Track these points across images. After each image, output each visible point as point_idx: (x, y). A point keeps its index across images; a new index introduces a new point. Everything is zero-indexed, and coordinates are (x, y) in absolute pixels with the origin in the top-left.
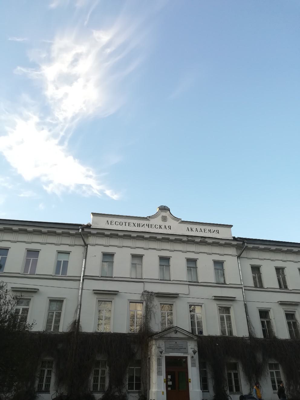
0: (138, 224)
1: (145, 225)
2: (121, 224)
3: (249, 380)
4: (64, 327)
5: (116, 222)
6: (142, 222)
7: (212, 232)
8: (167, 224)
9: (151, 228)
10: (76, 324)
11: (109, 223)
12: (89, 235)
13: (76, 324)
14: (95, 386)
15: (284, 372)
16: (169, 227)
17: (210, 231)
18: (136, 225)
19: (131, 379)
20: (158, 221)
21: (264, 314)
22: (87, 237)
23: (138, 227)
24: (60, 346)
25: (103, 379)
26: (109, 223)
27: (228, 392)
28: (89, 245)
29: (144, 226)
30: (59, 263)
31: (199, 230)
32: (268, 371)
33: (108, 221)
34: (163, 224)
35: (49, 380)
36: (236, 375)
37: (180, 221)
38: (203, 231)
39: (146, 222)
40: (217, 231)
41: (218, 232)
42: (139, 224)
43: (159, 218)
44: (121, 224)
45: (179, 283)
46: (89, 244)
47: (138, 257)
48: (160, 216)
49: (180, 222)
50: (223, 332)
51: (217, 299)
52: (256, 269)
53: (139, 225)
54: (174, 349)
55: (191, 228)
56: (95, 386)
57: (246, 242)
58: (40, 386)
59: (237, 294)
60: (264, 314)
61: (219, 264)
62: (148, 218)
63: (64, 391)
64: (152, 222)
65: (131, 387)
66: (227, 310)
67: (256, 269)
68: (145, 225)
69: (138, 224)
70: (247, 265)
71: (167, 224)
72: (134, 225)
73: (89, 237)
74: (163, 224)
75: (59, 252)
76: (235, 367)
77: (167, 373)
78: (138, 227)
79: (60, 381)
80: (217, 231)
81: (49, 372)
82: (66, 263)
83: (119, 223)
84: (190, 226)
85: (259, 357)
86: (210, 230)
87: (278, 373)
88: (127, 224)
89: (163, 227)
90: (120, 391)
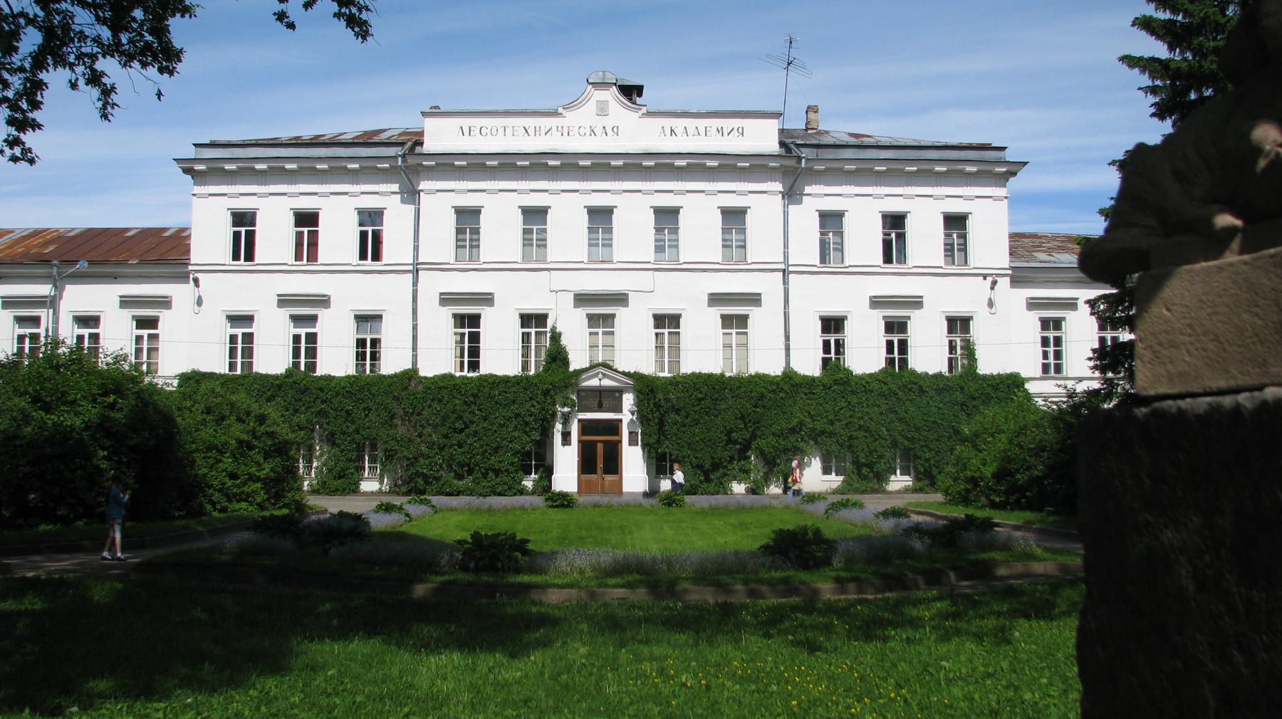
0: (535, 127)
1: (554, 129)
2: (494, 131)
5: (481, 128)
7: (725, 134)
8: (609, 122)
9: (568, 135)
11: (466, 131)
12: (419, 169)
16: (615, 129)
17: (720, 131)
18: (531, 131)
21: (832, 324)
22: (418, 173)
23: (535, 135)
26: (466, 131)
28: (421, 193)
29: (550, 132)
31: (691, 131)
33: (461, 128)
34: (598, 123)
37: (644, 110)
38: (702, 133)
40: (740, 130)
41: (743, 134)
42: (538, 129)
44: (494, 131)
46: (422, 191)
47: (534, 215)
49: (643, 114)
51: (716, 299)
52: (831, 221)
55: (671, 128)
57: (804, 158)
59: (768, 286)
61: (734, 217)
62: (560, 110)
67: (831, 221)
68: (554, 129)
69: (535, 127)
70: (805, 217)
71: (609, 122)
72: (527, 132)
73: (422, 174)
74: (598, 123)
78: (535, 135)
80: (740, 130)
83: (489, 129)
84: (669, 122)
86: (722, 128)
88: (509, 131)
89: (598, 130)
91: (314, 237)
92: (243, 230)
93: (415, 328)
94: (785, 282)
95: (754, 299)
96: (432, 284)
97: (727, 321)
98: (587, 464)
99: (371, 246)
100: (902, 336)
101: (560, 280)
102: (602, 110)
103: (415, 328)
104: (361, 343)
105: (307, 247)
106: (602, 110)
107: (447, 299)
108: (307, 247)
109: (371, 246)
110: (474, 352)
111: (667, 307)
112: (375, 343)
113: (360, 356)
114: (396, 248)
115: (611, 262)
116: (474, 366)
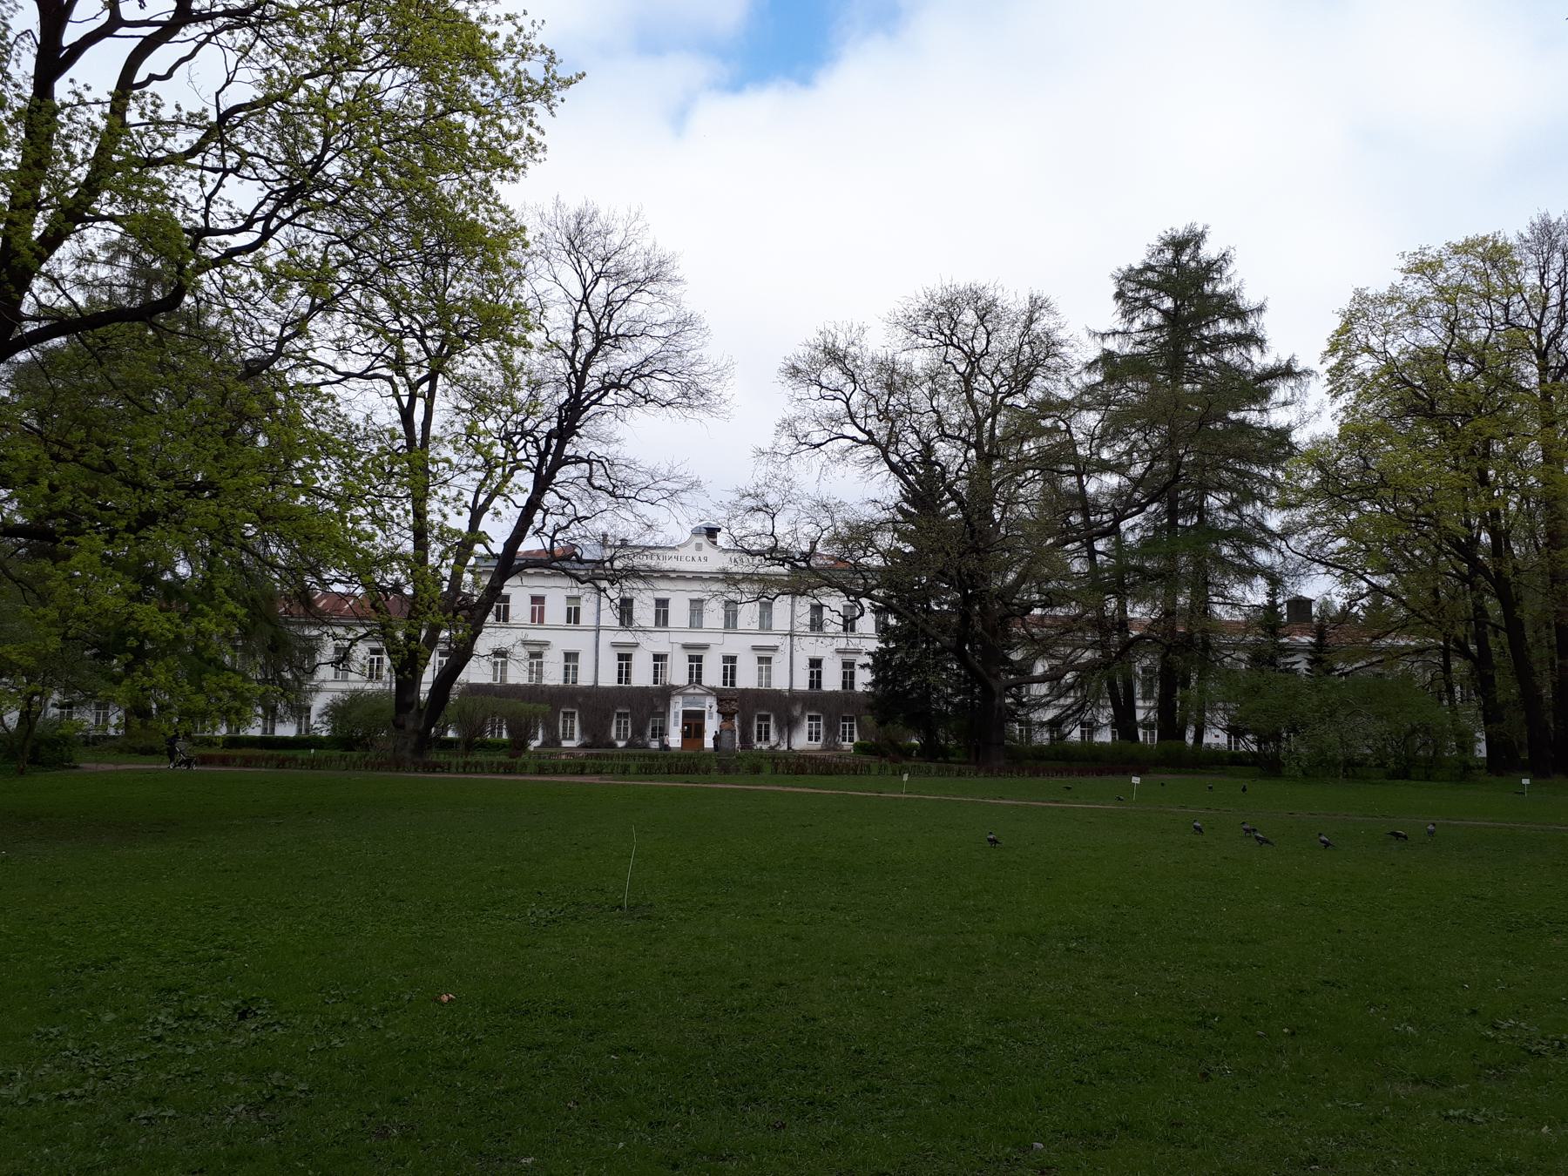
3: (780, 731)
8: (702, 554)
15: (825, 724)
19: (654, 729)
20: (690, 551)
21: (816, 663)
25: (626, 729)
27: (755, 740)
30: (569, 610)
32: (806, 723)
34: (697, 554)
35: (572, 729)
36: (767, 727)
43: (693, 545)
45: (713, 631)
48: (694, 543)
50: (760, 684)
51: (755, 648)
54: (691, 704)
58: (564, 734)
60: (816, 663)
63: (587, 739)
64: (682, 552)
65: (654, 736)
66: (769, 660)
71: (702, 554)
74: (697, 554)
75: (568, 598)
76: (767, 718)
77: (684, 725)
79: (583, 731)
81: (572, 722)
82: (577, 610)
85: (797, 712)
87: (818, 726)
90: (643, 739)
91: (542, 610)
93: (597, 660)
94: (792, 641)
95: (775, 649)
96: (606, 638)
97: (760, 660)
98: (685, 735)
99: (573, 616)
101: (676, 638)
102: (699, 547)
103: (597, 660)
104: (567, 668)
105: (538, 615)
106: (699, 547)
107: (615, 645)
108: (538, 615)
109: (573, 616)
111: (731, 652)
112: (575, 668)
113: (566, 675)
114: (587, 617)
115: (701, 628)
116: (628, 681)
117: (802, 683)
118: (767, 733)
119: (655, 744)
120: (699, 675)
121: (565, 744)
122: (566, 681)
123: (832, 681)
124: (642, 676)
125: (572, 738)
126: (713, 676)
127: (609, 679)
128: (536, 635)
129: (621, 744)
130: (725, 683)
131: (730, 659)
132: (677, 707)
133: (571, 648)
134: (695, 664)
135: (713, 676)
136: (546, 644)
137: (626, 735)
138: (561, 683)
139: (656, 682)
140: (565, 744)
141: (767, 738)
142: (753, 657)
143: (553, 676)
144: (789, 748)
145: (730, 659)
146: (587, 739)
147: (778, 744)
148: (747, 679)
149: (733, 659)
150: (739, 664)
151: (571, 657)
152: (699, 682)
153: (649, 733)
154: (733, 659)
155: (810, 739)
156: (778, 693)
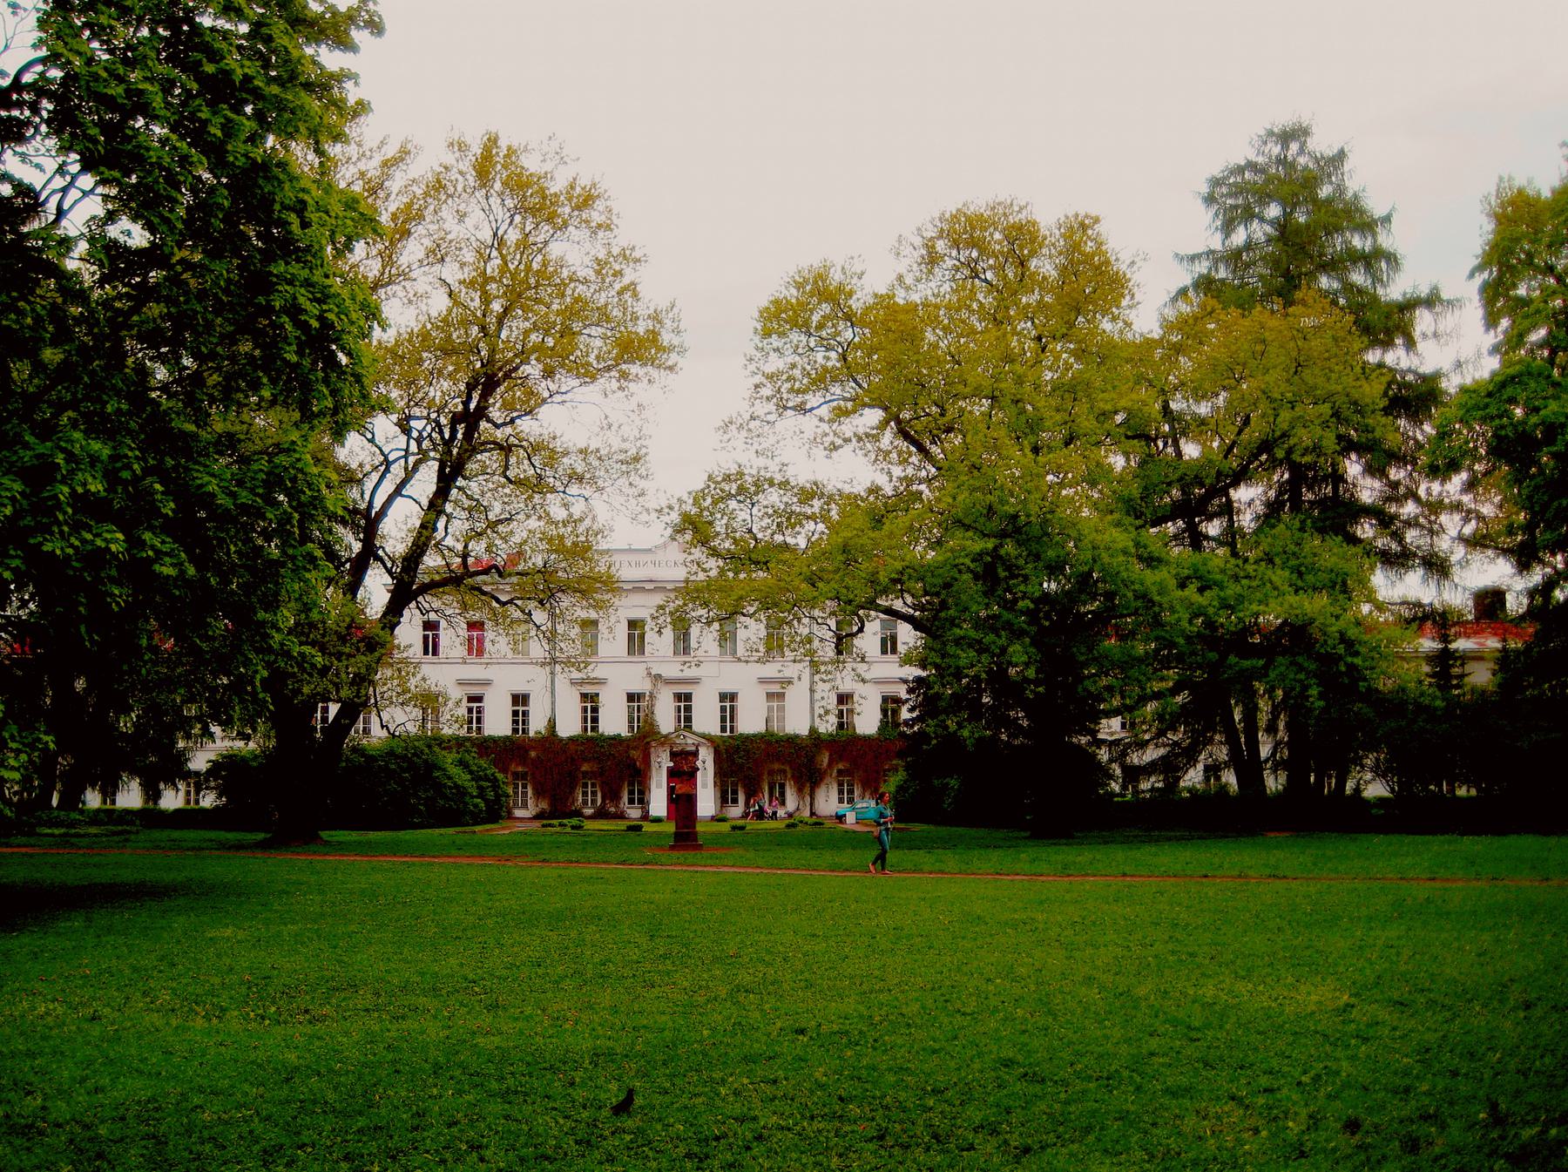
3: (800, 791)
4: (537, 725)
6: (643, 558)
10: (552, 724)
13: (552, 724)
14: (585, 802)
24: (533, 754)
35: (525, 794)
36: (782, 787)
39: (649, 557)
53: (637, 564)
56: (585, 802)
63: (544, 805)
64: (660, 556)
65: (631, 801)
66: (781, 696)
79: (538, 794)
81: (524, 786)
90: (617, 806)
92: (430, 633)
93: (553, 703)
97: (770, 696)
100: (849, 707)
103: (553, 703)
104: (515, 713)
110: (595, 720)
111: (728, 688)
112: (525, 714)
113: (515, 722)
117: (827, 726)
118: (782, 794)
119: (634, 813)
120: (688, 719)
121: (518, 813)
122: (515, 731)
123: (867, 722)
124: (614, 722)
125: (525, 806)
126: (707, 720)
127: (569, 727)
128: (475, 671)
129: (589, 811)
130: (723, 729)
131: (728, 698)
132: (661, 764)
133: (520, 688)
134: (682, 704)
135: (707, 720)
136: (487, 683)
137: (593, 802)
138: (509, 733)
139: (631, 728)
140: (518, 813)
141: (783, 803)
142: (760, 693)
143: (497, 724)
144: (813, 814)
145: (728, 698)
146: (544, 805)
147: (798, 809)
148: (751, 722)
149: (732, 697)
150: (741, 704)
151: (520, 699)
152: (688, 727)
153: (625, 798)
154: (732, 697)
155: (841, 801)
156: (792, 740)
